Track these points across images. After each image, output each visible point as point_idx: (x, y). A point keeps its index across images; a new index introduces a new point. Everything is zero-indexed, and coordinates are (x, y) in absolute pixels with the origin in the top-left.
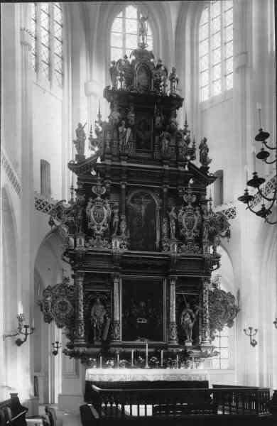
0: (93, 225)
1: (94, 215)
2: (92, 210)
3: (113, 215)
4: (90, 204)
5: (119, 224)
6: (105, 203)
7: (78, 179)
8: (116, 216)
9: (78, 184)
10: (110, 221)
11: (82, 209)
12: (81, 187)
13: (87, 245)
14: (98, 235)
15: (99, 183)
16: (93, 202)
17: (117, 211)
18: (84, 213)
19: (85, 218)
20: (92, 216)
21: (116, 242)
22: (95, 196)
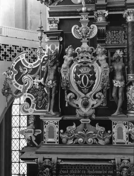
0: (76, 98)
1: (77, 79)
2: (73, 68)
3: (112, 75)
4: (67, 58)
5: (125, 90)
6: (95, 55)
7: (51, 14)
8: (119, 76)
9: (50, 22)
10: (108, 90)
11: (55, 67)
12: (55, 26)
13: (64, 136)
14: (85, 117)
15: (84, 18)
16: (74, 55)
17: (118, 66)
18: (58, 76)
19: (58, 86)
20: (73, 80)
21: (120, 130)
22: (77, 43)
